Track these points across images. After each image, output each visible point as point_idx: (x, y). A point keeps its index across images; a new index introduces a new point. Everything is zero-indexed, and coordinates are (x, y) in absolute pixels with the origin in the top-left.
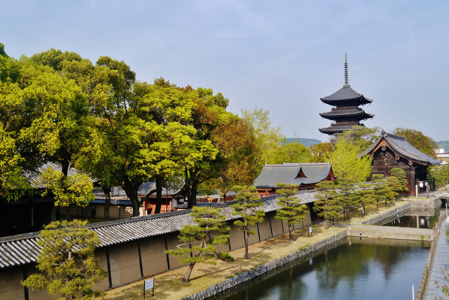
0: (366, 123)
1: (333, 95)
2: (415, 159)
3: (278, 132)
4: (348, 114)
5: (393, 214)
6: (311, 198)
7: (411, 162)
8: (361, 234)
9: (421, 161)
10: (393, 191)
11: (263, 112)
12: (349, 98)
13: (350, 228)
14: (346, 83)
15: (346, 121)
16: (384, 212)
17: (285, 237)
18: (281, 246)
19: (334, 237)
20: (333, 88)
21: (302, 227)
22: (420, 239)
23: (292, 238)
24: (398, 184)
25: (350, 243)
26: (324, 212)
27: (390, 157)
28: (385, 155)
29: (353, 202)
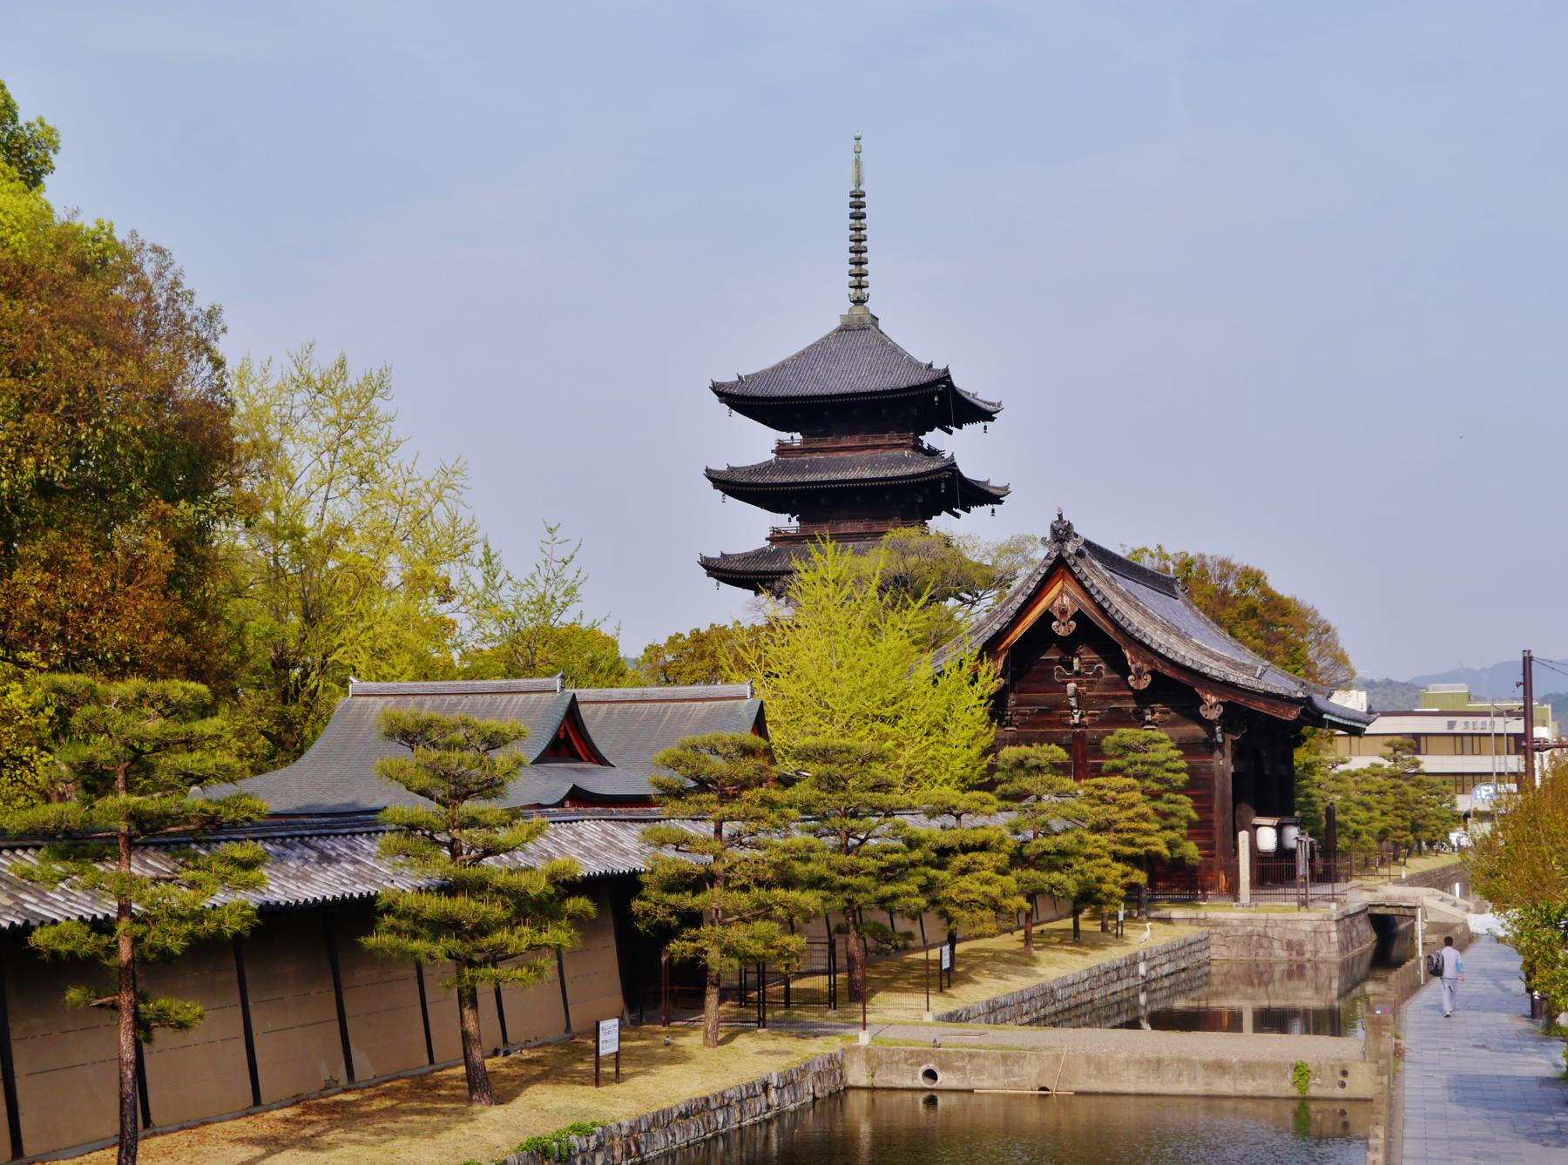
1: (783, 365)
2: (1233, 686)
3: (438, 499)
4: (867, 474)
5: (1117, 987)
6: (624, 853)
7: (1211, 699)
8: (931, 1075)
9: (1268, 695)
10: (1117, 857)
11: (354, 378)
12: (872, 387)
13: (864, 1038)
14: (859, 302)
16: (1060, 967)
17: (437, 1085)
18: (396, 1133)
19: (766, 1087)
20: (783, 330)
21: (557, 1033)
22: (1287, 1088)
23: (482, 1087)
24: (1143, 817)
25: (865, 1129)
26: (706, 929)
27: (1098, 673)
28: (1069, 666)
29: (887, 890)
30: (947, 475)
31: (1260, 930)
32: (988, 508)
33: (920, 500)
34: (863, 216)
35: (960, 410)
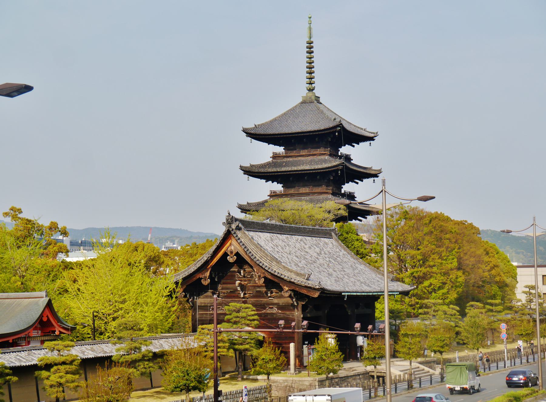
0: (362, 191)
1: (275, 120)
4: (307, 167)
15: (304, 186)
30: (341, 167)
31: (290, 384)
32: (372, 179)
33: (332, 178)
34: (312, 52)
35: (356, 138)
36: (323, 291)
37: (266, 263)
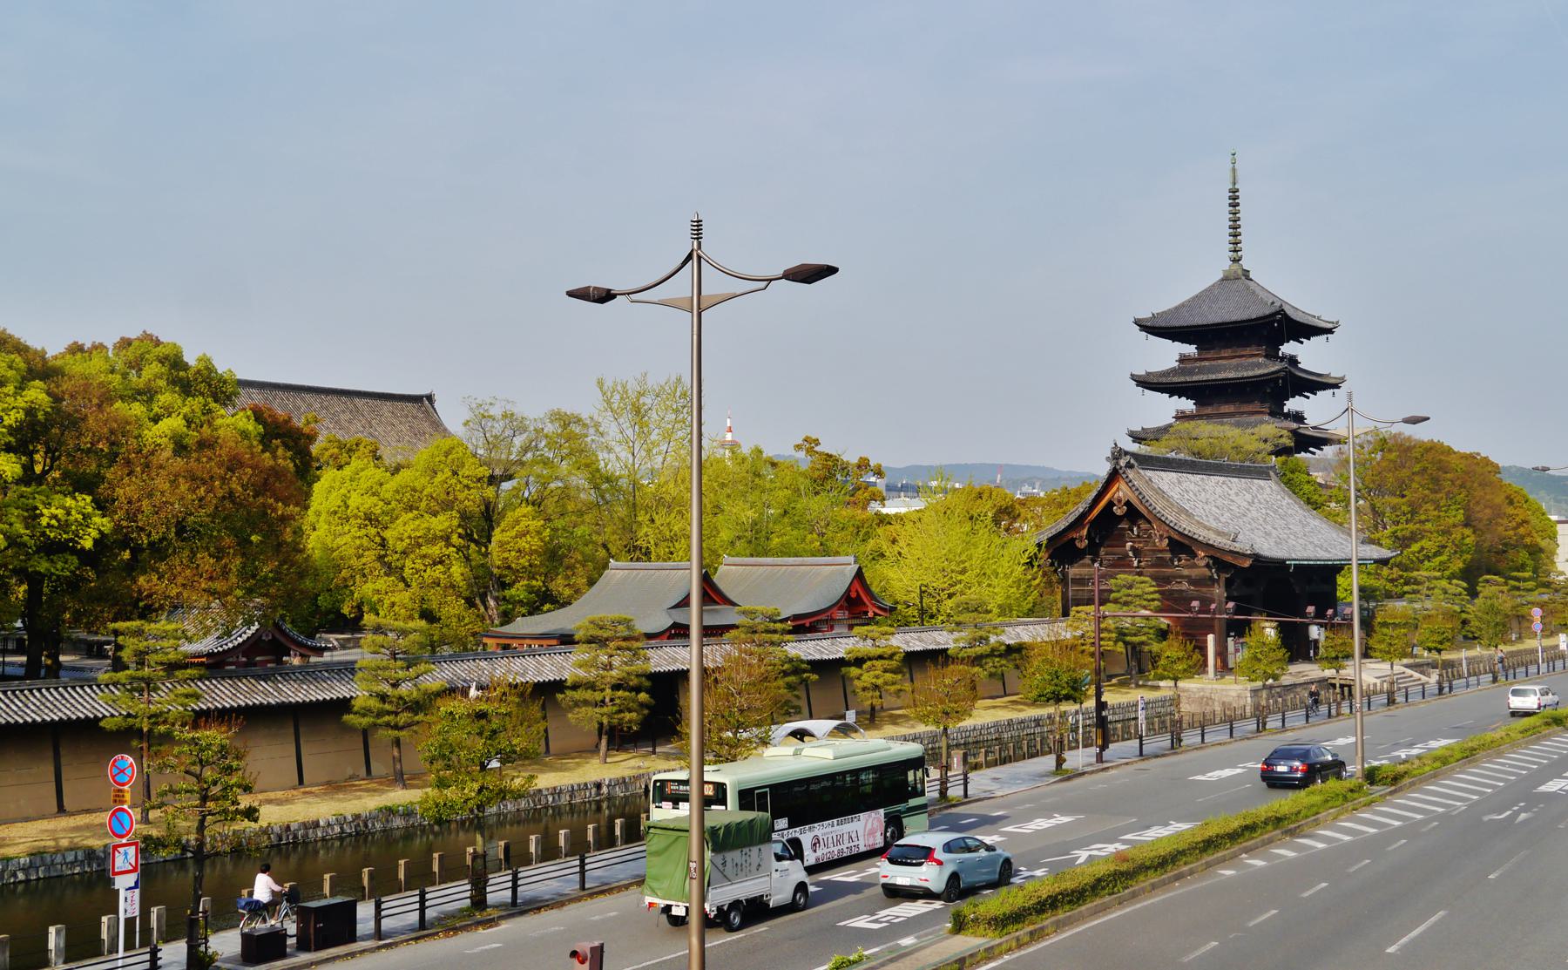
0: (1314, 409)
1: (1183, 305)
4: (1232, 375)
12: (1234, 318)
14: (1236, 261)
15: (1227, 402)
20: (1186, 278)
35: (1305, 331)
36: (1257, 558)
37: (1171, 517)
